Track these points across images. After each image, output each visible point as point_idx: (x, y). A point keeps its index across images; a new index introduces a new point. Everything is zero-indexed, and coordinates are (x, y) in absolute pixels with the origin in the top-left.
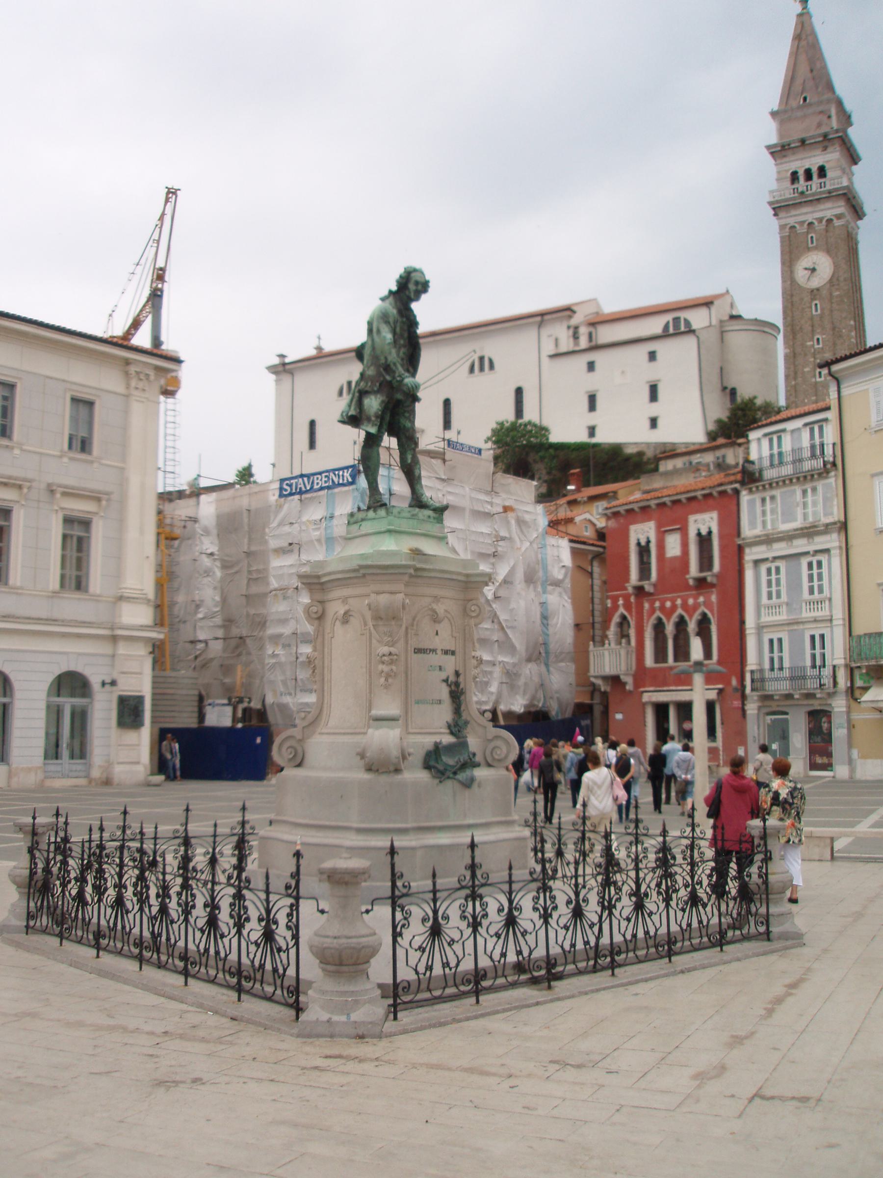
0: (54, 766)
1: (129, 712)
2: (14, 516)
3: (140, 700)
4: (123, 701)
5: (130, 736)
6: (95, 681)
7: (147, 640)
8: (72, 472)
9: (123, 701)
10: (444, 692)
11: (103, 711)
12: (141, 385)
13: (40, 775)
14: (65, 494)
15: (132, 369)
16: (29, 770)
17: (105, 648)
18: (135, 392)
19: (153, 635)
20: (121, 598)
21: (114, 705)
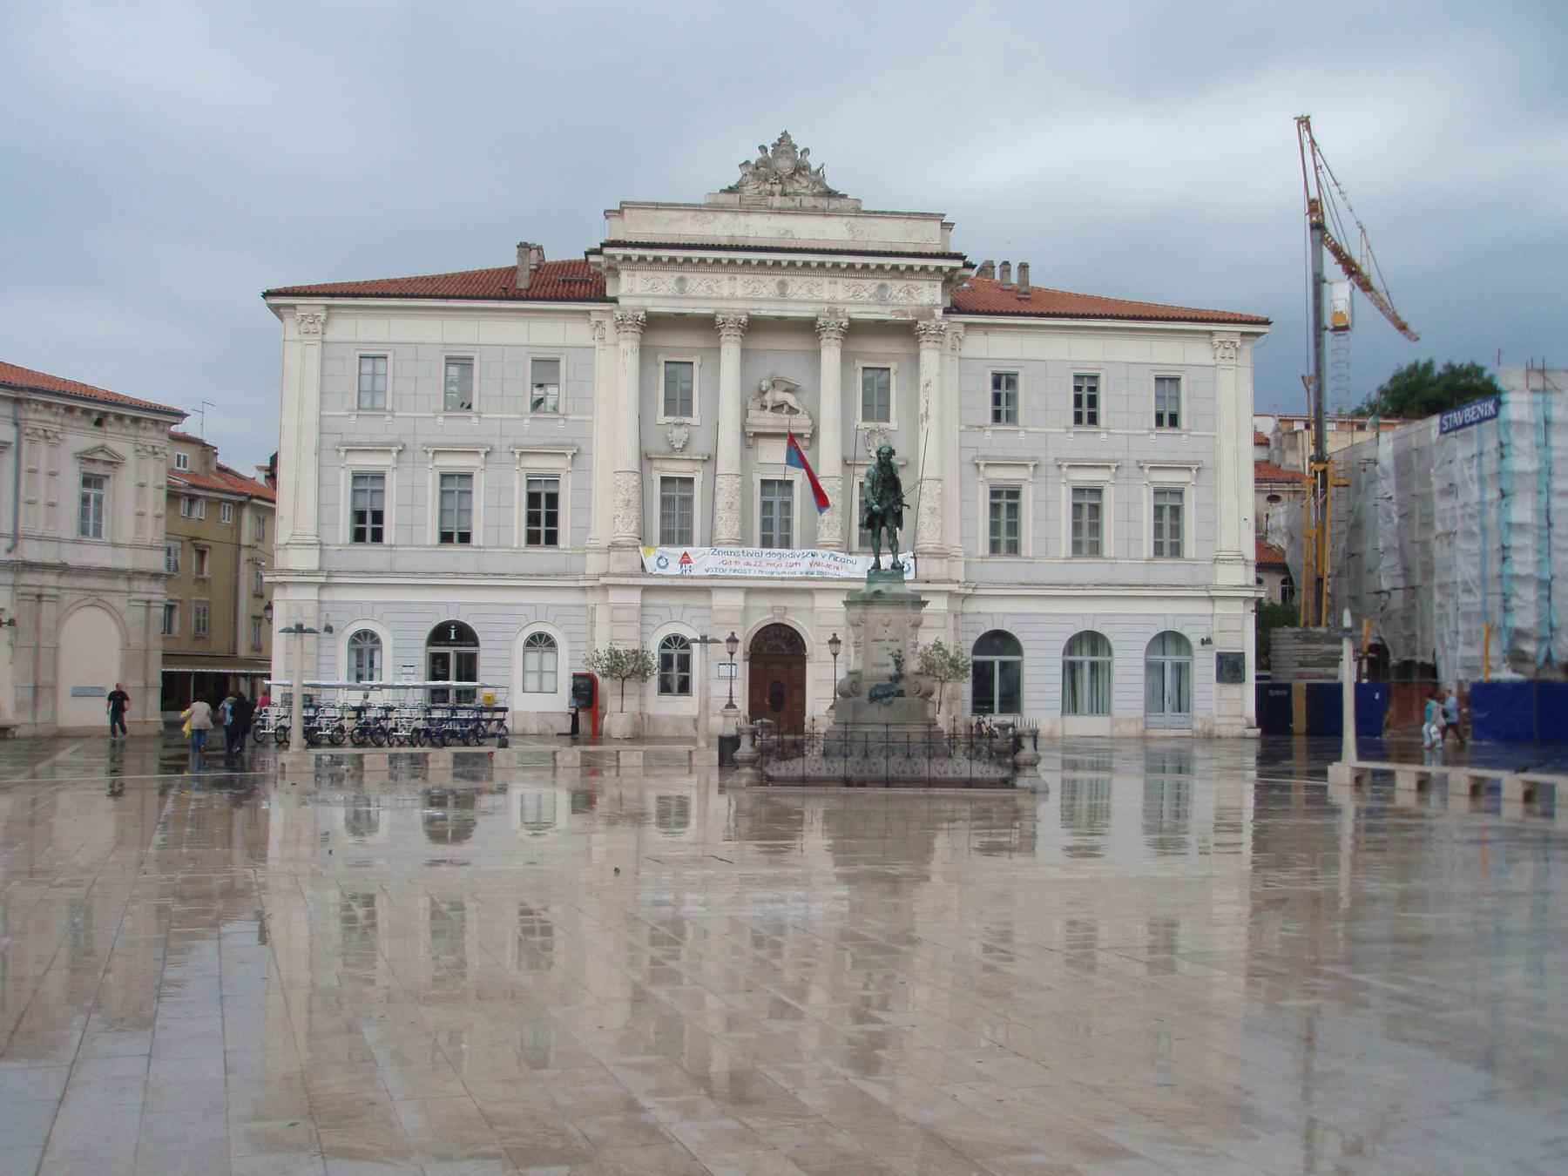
0: (1155, 719)
1: (1229, 668)
2: (1105, 493)
3: (1241, 656)
4: (1221, 657)
5: (1232, 691)
6: (1194, 640)
7: (1247, 599)
8: (1163, 445)
9: (1221, 657)
10: (891, 660)
11: (1203, 667)
12: (1227, 353)
13: (1141, 726)
14: (1152, 468)
15: (1216, 340)
16: (1130, 720)
17: (1205, 608)
18: (1222, 362)
19: (1252, 594)
20: (1216, 560)
21: (1214, 662)
